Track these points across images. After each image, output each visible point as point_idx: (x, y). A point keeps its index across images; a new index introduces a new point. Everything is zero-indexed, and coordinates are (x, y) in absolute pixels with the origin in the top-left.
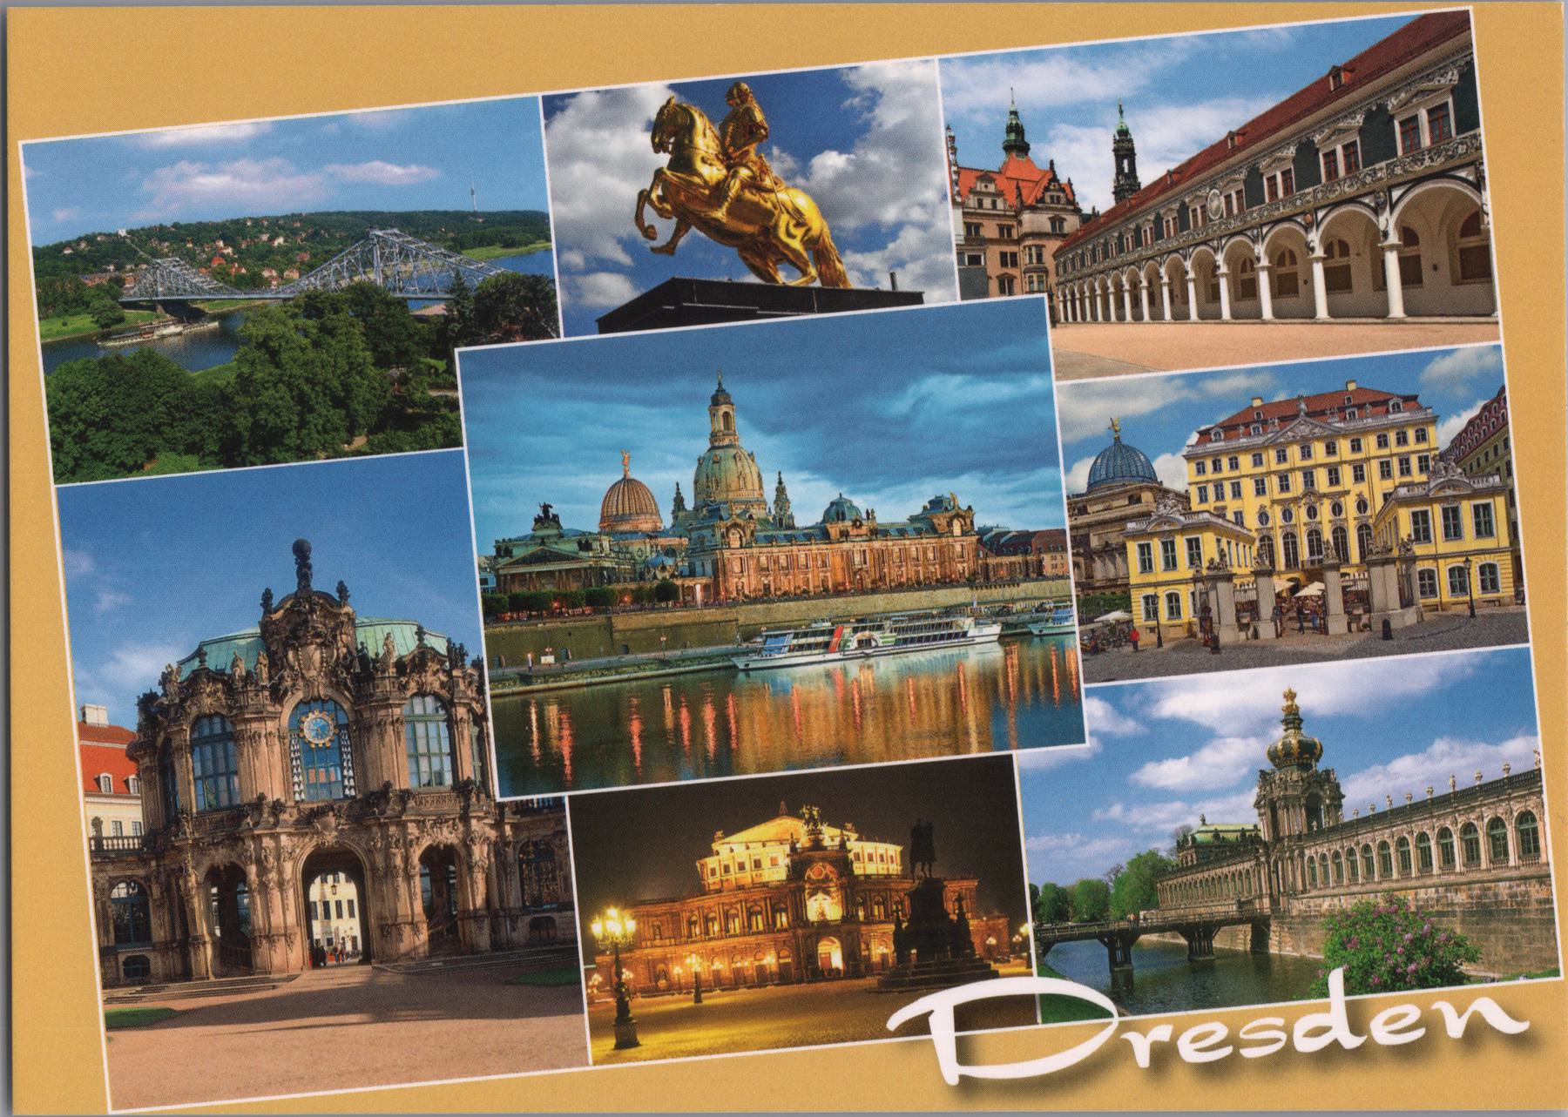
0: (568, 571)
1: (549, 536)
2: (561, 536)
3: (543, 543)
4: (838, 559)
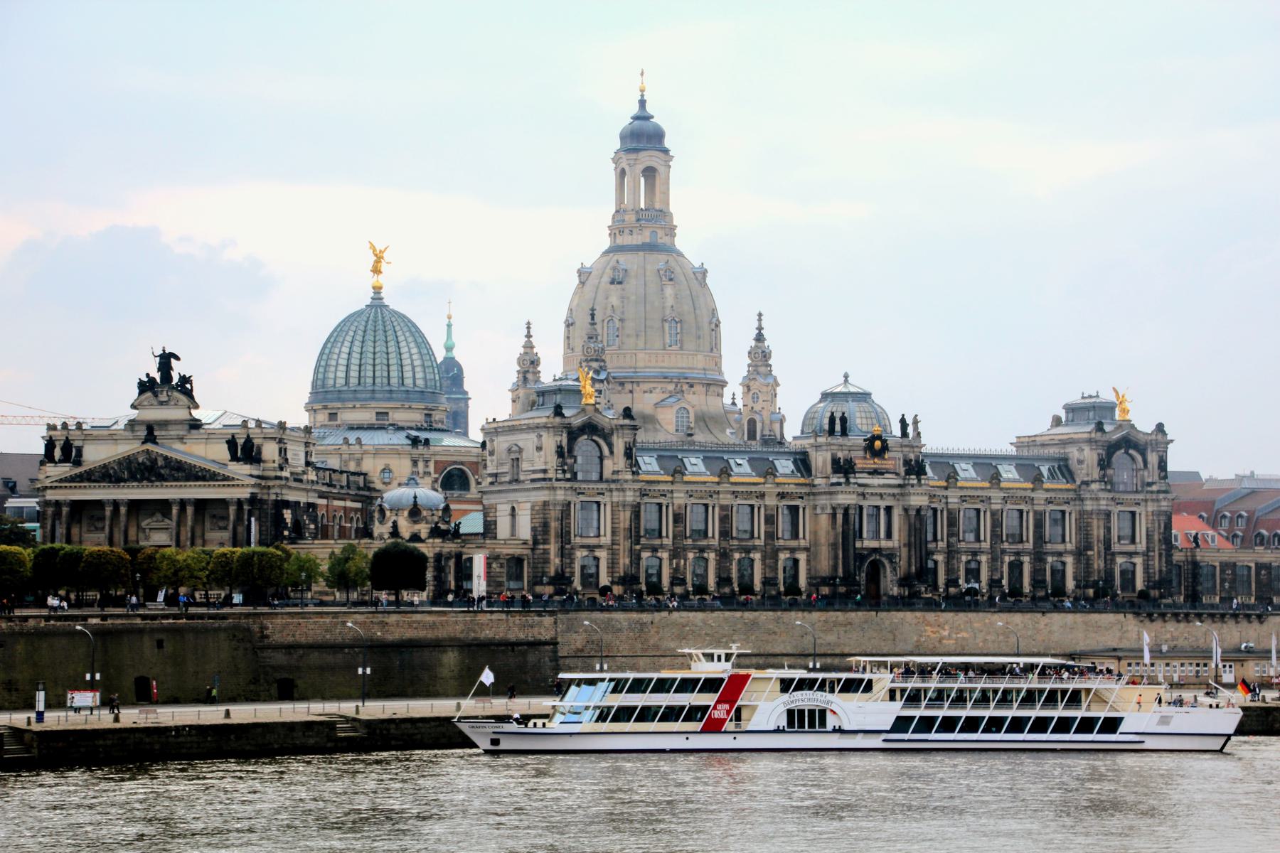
0: (201, 505)
1: (165, 424)
2: (195, 425)
3: (150, 438)
4: (824, 520)
